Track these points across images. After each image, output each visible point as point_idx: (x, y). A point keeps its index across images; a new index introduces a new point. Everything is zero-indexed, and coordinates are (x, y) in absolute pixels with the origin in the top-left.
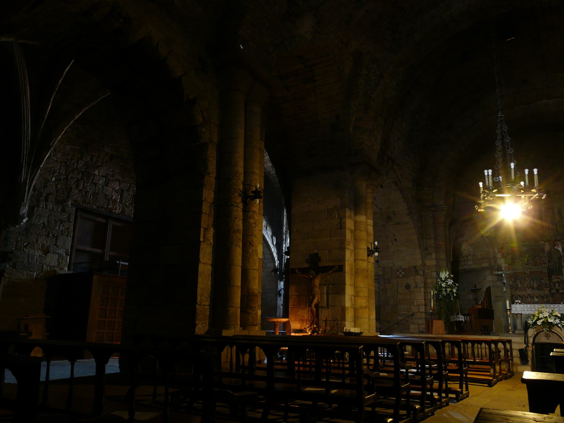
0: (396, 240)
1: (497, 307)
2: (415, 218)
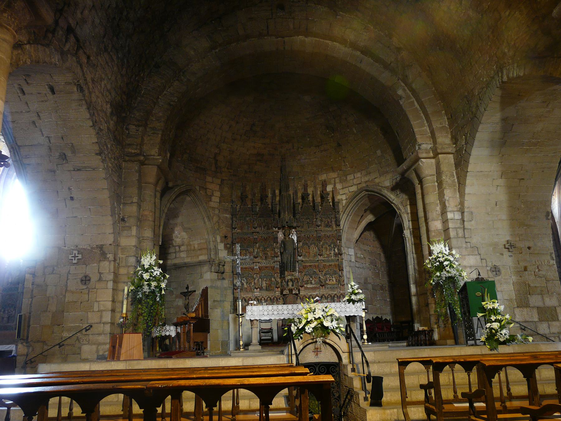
1: (215, 315)
2: (110, 165)
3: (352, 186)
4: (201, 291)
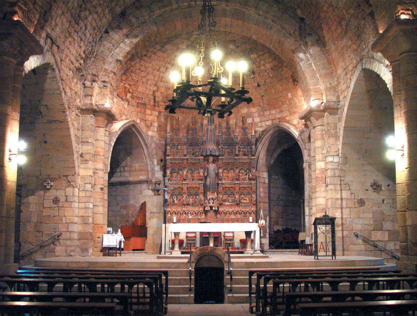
0: (45, 142)
3: (268, 121)
4: (140, 204)
